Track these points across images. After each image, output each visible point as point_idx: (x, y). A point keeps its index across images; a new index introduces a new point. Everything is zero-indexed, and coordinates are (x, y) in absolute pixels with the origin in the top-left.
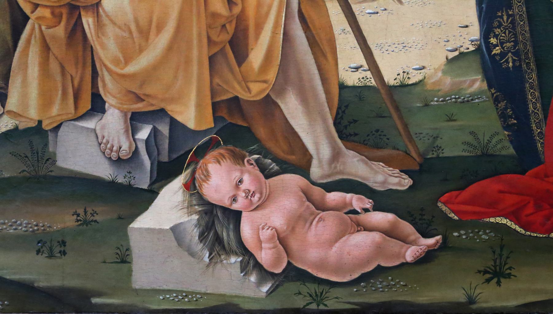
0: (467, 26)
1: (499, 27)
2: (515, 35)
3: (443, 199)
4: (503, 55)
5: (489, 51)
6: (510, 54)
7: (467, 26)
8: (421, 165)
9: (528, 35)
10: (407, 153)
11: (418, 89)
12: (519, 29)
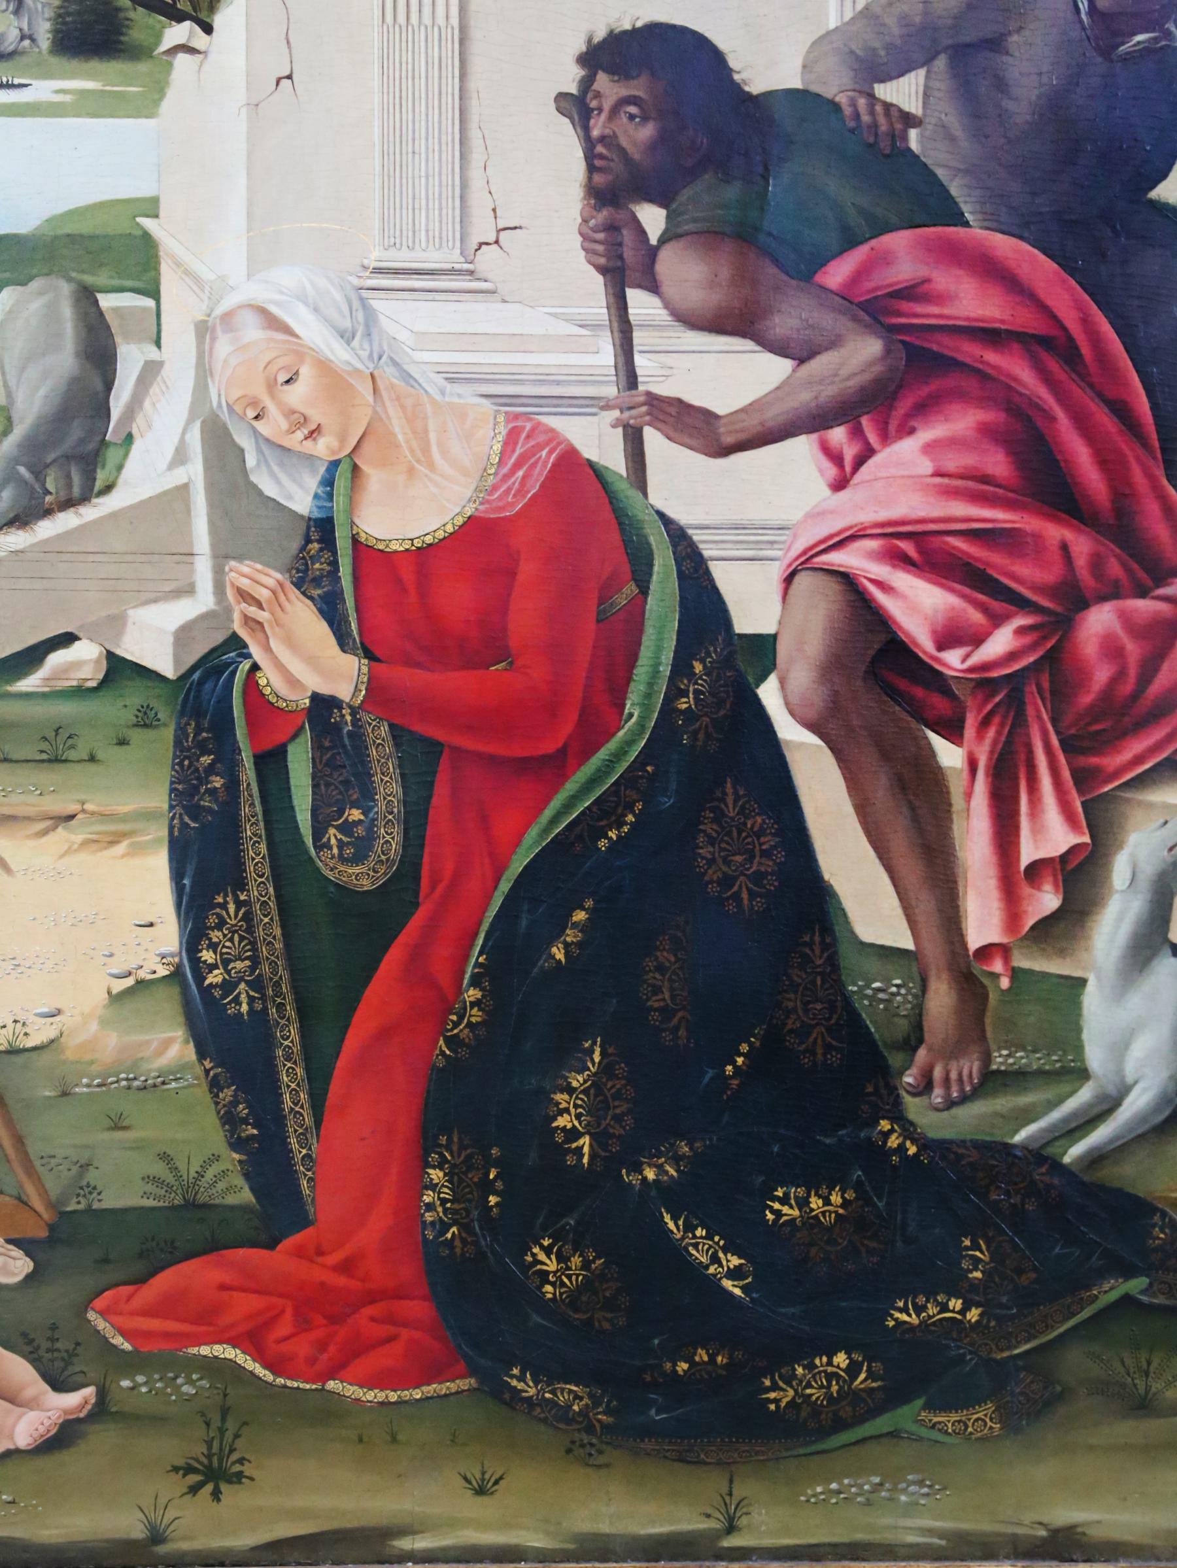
0: (151, 925)
1: (220, 926)
2: (253, 943)
3: (99, 1303)
4: (228, 986)
5: (199, 978)
6: (242, 986)
7: (151, 925)
8: (52, 1228)
9: (279, 945)
10: (22, 1201)
11: (44, 1059)
12: (260, 932)
